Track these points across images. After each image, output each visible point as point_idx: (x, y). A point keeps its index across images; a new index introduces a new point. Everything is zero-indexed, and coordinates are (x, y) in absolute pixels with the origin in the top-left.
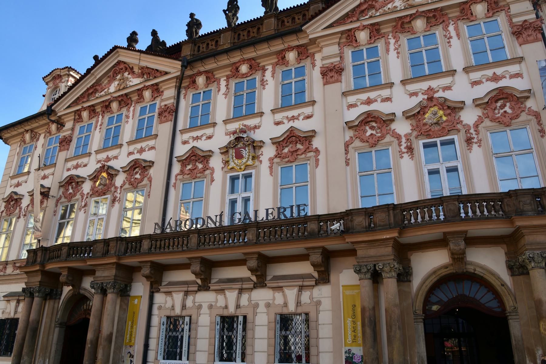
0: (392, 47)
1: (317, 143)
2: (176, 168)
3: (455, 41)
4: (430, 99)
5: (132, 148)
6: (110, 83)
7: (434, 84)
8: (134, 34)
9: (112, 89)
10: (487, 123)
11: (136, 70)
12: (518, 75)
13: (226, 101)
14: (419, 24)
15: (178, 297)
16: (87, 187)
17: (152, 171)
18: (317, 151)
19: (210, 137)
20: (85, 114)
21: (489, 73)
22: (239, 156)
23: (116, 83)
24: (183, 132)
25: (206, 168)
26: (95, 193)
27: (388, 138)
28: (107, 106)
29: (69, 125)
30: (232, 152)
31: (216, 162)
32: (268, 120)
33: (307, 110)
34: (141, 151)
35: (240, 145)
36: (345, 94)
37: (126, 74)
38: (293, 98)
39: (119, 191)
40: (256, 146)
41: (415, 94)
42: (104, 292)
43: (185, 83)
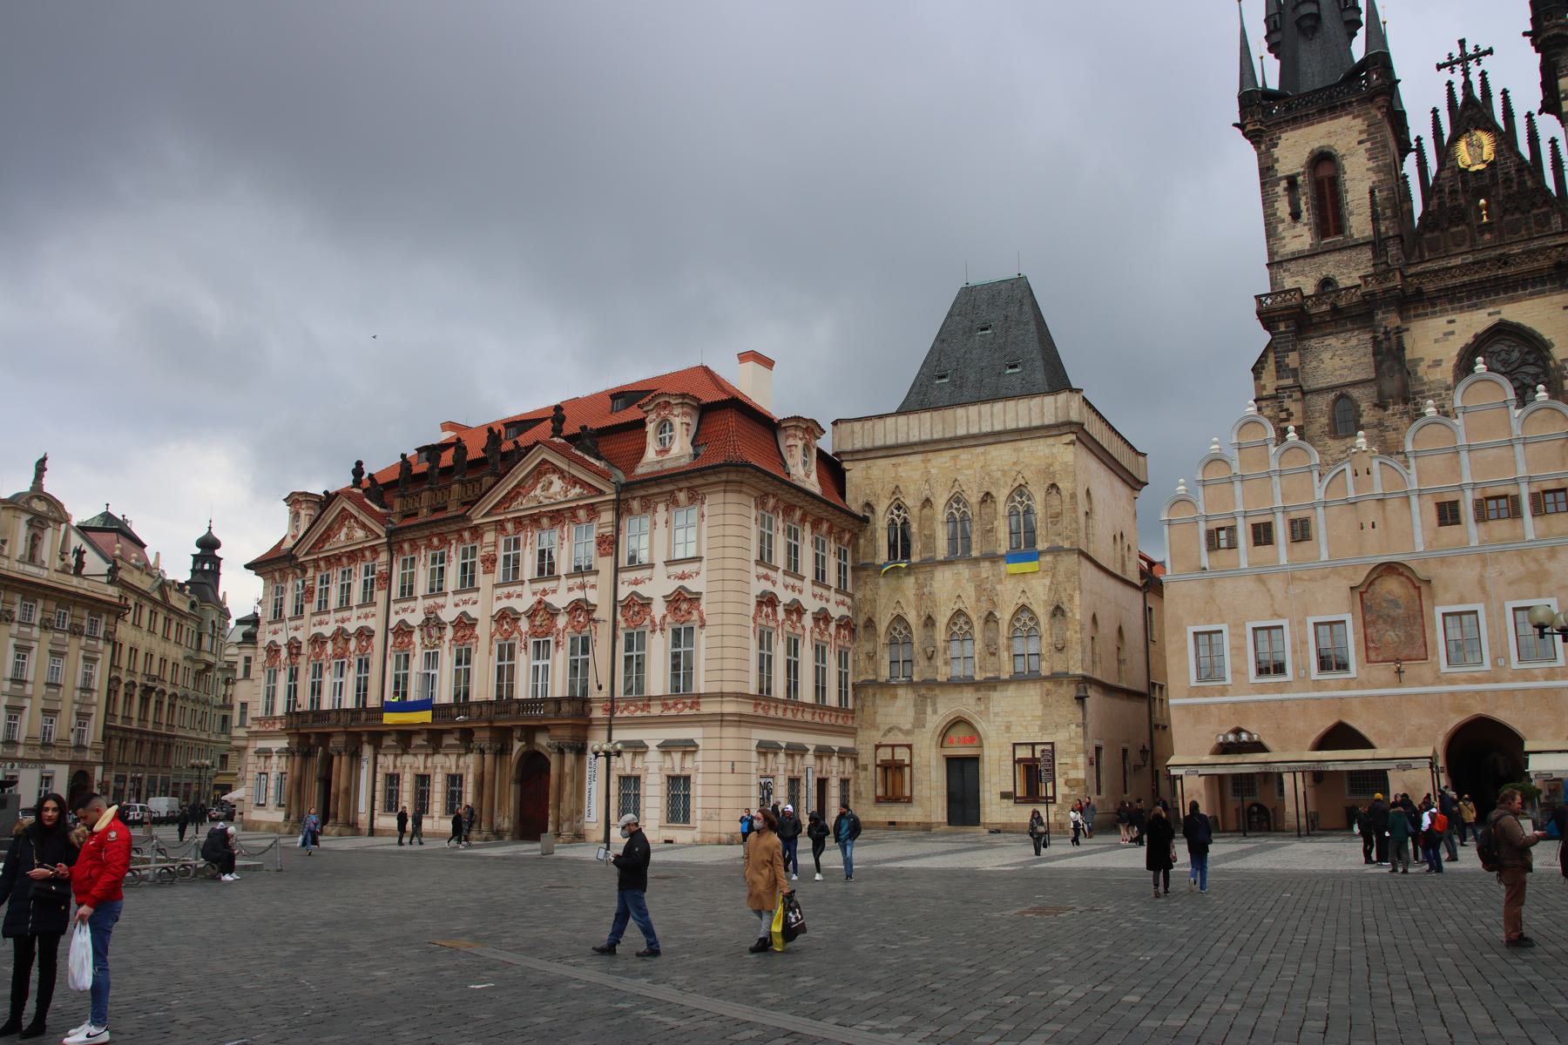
1: (478, 630)
4: (540, 602)
6: (340, 529)
8: (359, 464)
9: (343, 537)
10: (569, 629)
14: (545, 521)
15: (391, 758)
16: (329, 647)
20: (322, 564)
22: (430, 636)
24: (396, 601)
25: (410, 643)
26: (335, 656)
27: (516, 634)
28: (338, 558)
29: (310, 573)
32: (450, 600)
33: (474, 596)
34: (366, 617)
36: (497, 586)
38: (468, 581)
40: (441, 626)
41: (534, 594)
42: (340, 754)
43: (395, 547)
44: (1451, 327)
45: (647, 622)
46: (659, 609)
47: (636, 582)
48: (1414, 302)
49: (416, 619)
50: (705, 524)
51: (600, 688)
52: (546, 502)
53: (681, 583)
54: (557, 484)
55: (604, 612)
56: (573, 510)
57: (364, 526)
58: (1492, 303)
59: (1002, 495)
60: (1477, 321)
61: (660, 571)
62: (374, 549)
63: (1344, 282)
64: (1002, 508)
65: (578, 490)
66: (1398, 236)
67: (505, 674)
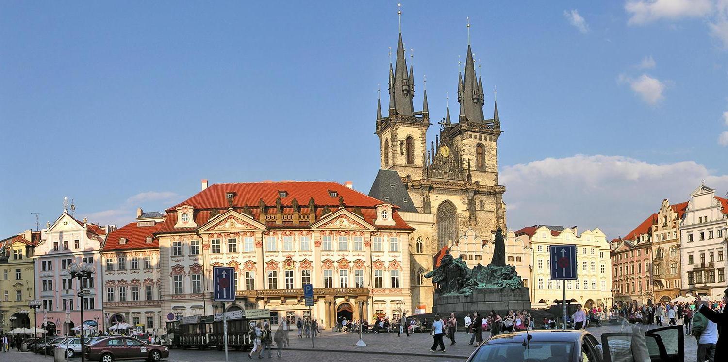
0: (335, 239)
1: (312, 265)
2: (266, 265)
3: (351, 241)
5: (245, 255)
7: (345, 253)
10: (355, 267)
11: (240, 220)
12: (363, 256)
13: (281, 243)
17: (256, 266)
18: (312, 267)
19: (277, 256)
21: (357, 253)
23: (229, 223)
25: (277, 267)
27: (332, 267)
30: (286, 263)
31: (280, 265)
32: (297, 254)
33: (309, 253)
34: (249, 257)
35: (289, 261)
37: (234, 220)
39: (242, 271)
41: (339, 255)
44: (437, 198)
45: (383, 267)
46: (387, 265)
47: (378, 256)
48: (431, 188)
49: (281, 258)
50: (401, 243)
51: (369, 285)
52: (342, 227)
53: (394, 258)
54: (346, 223)
55: (367, 264)
56: (355, 232)
57: (244, 222)
58: (446, 194)
59: (416, 238)
60: (442, 198)
61: (386, 254)
62: (252, 233)
63: (413, 178)
64: (416, 243)
65: (355, 225)
66: (427, 170)
67: (328, 282)
